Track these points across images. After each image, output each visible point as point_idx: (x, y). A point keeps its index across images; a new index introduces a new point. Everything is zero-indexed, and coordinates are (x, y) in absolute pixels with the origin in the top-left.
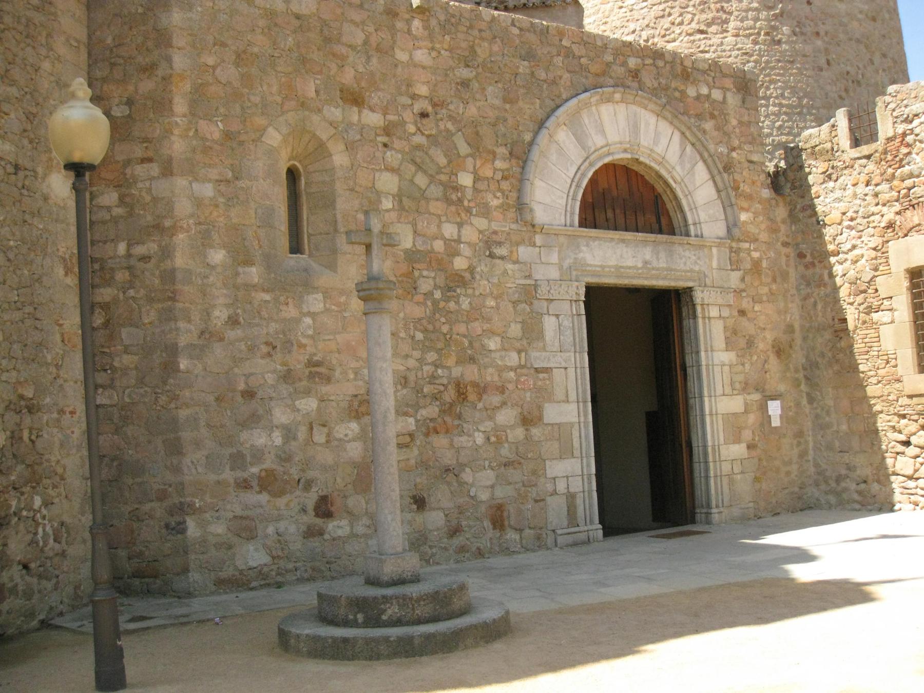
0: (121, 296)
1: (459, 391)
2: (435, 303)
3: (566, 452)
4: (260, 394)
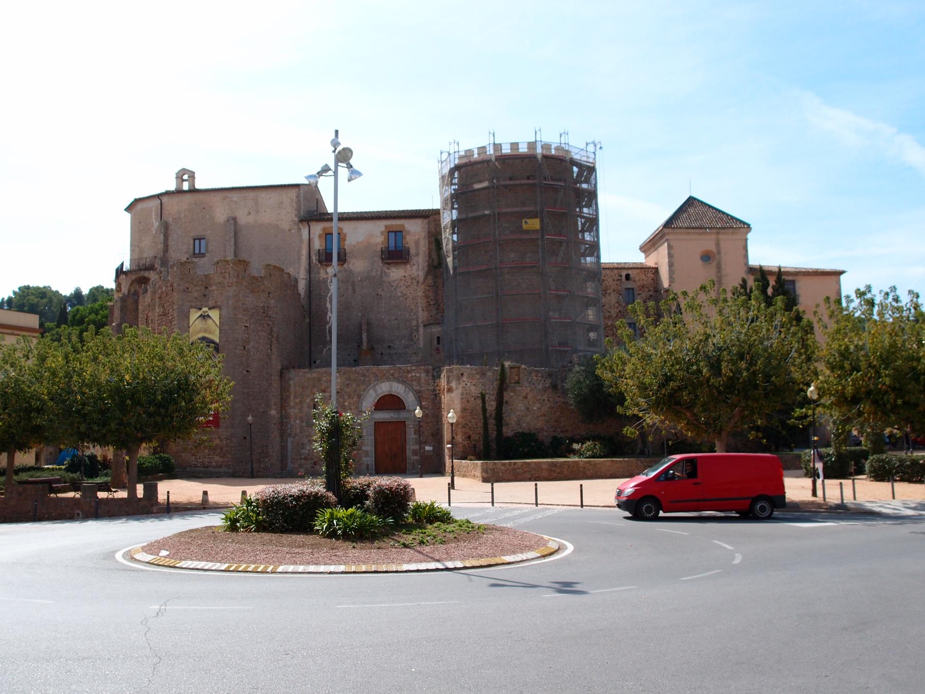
3: (367, 455)
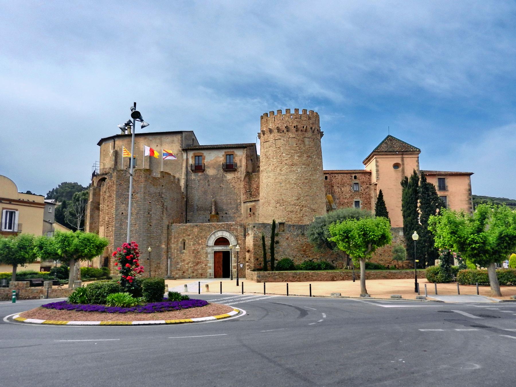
3: (210, 268)
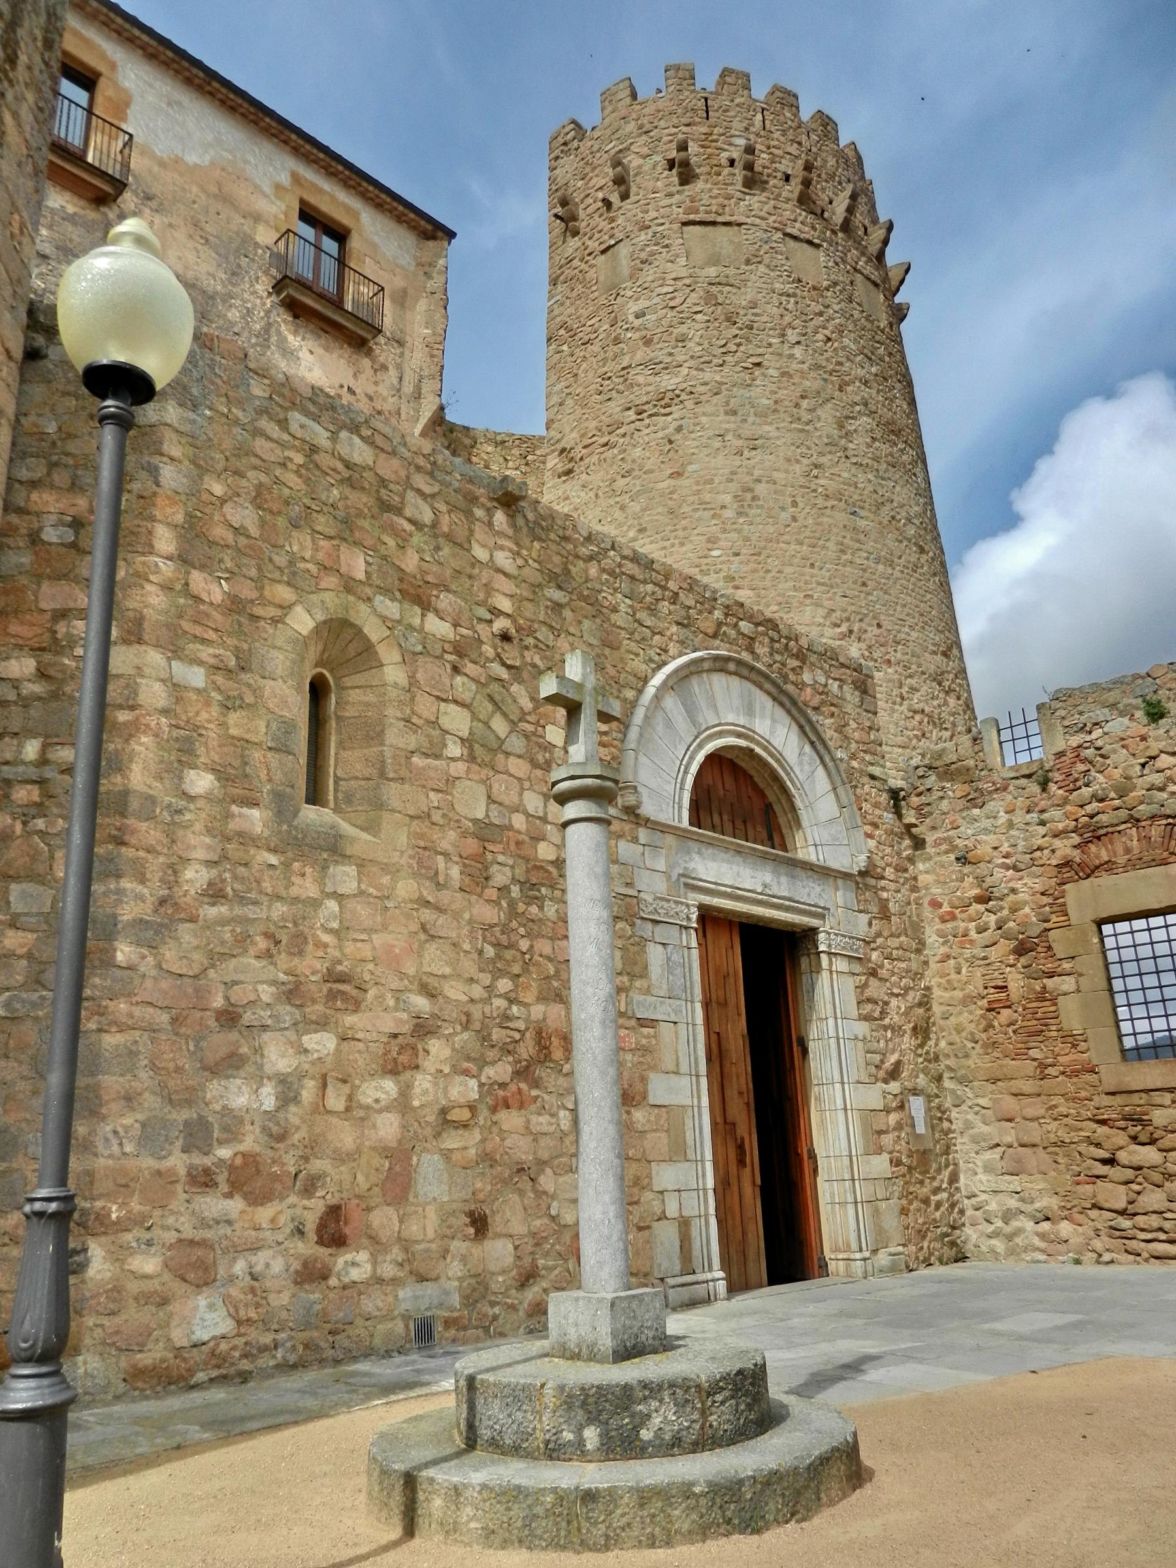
0: (18, 828)
1: (539, 1043)
2: (512, 904)
4: (248, 1017)
